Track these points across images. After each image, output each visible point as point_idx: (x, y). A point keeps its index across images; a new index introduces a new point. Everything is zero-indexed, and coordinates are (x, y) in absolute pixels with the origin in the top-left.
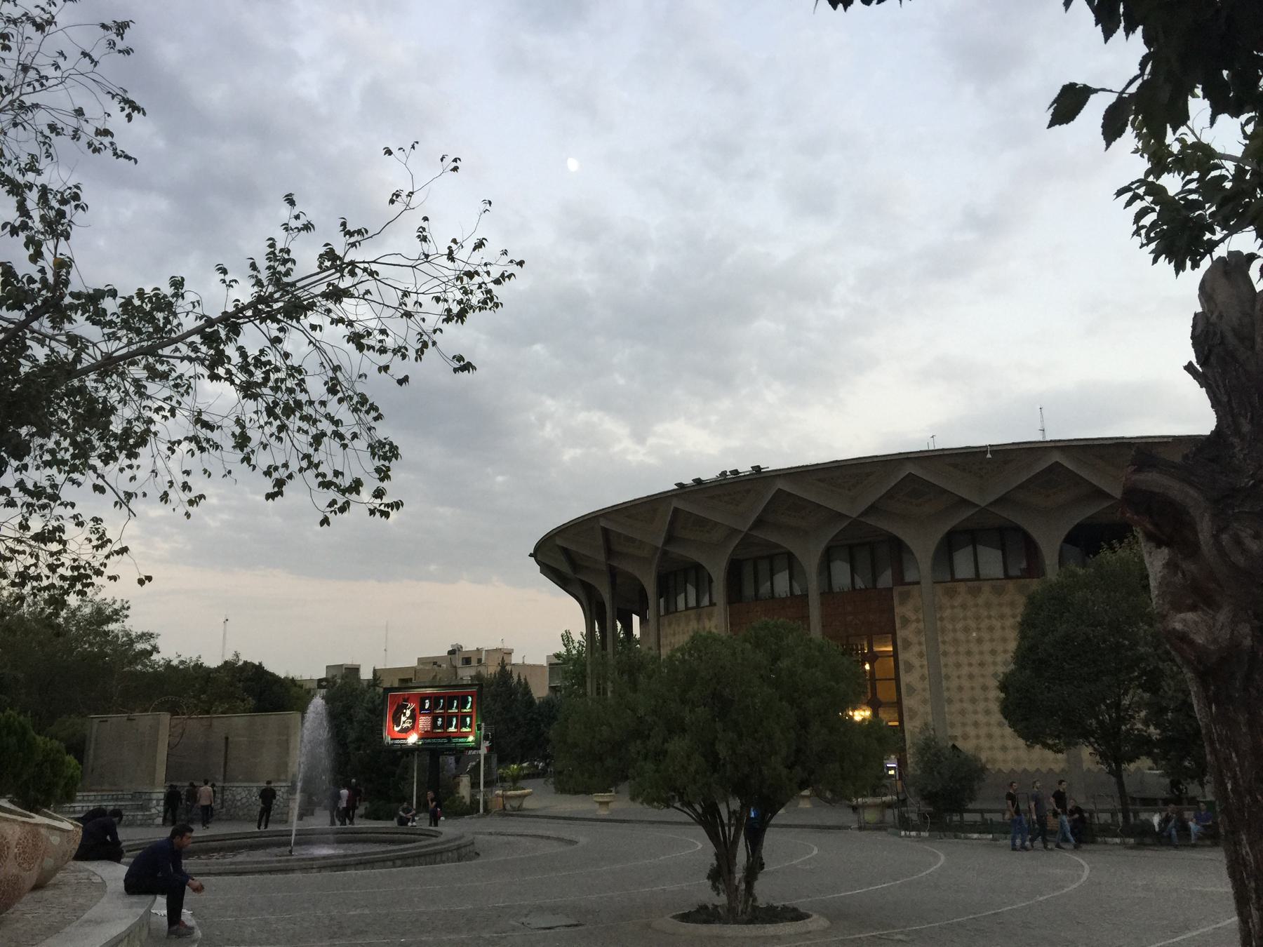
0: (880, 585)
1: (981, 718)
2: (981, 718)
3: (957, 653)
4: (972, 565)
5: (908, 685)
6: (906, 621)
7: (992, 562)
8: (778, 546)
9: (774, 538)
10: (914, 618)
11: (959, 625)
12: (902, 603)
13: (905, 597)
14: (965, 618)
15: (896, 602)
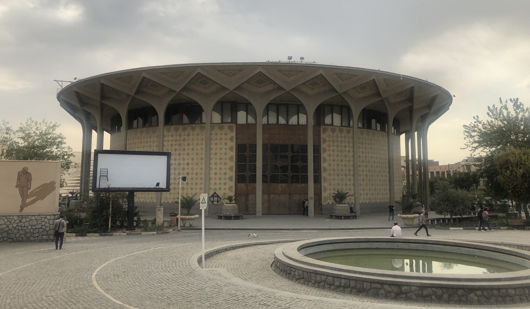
0: (290, 123)
1: (348, 182)
2: (348, 182)
3: (342, 156)
4: (331, 119)
5: (324, 168)
6: (325, 141)
7: (337, 119)
8: (300, 101)
9: (296, 95)
10: (328, 140)
11: (343, 145)
12: (324, 132)
13: (325, 131)
14: (345, 142)
15: (321, 133)
